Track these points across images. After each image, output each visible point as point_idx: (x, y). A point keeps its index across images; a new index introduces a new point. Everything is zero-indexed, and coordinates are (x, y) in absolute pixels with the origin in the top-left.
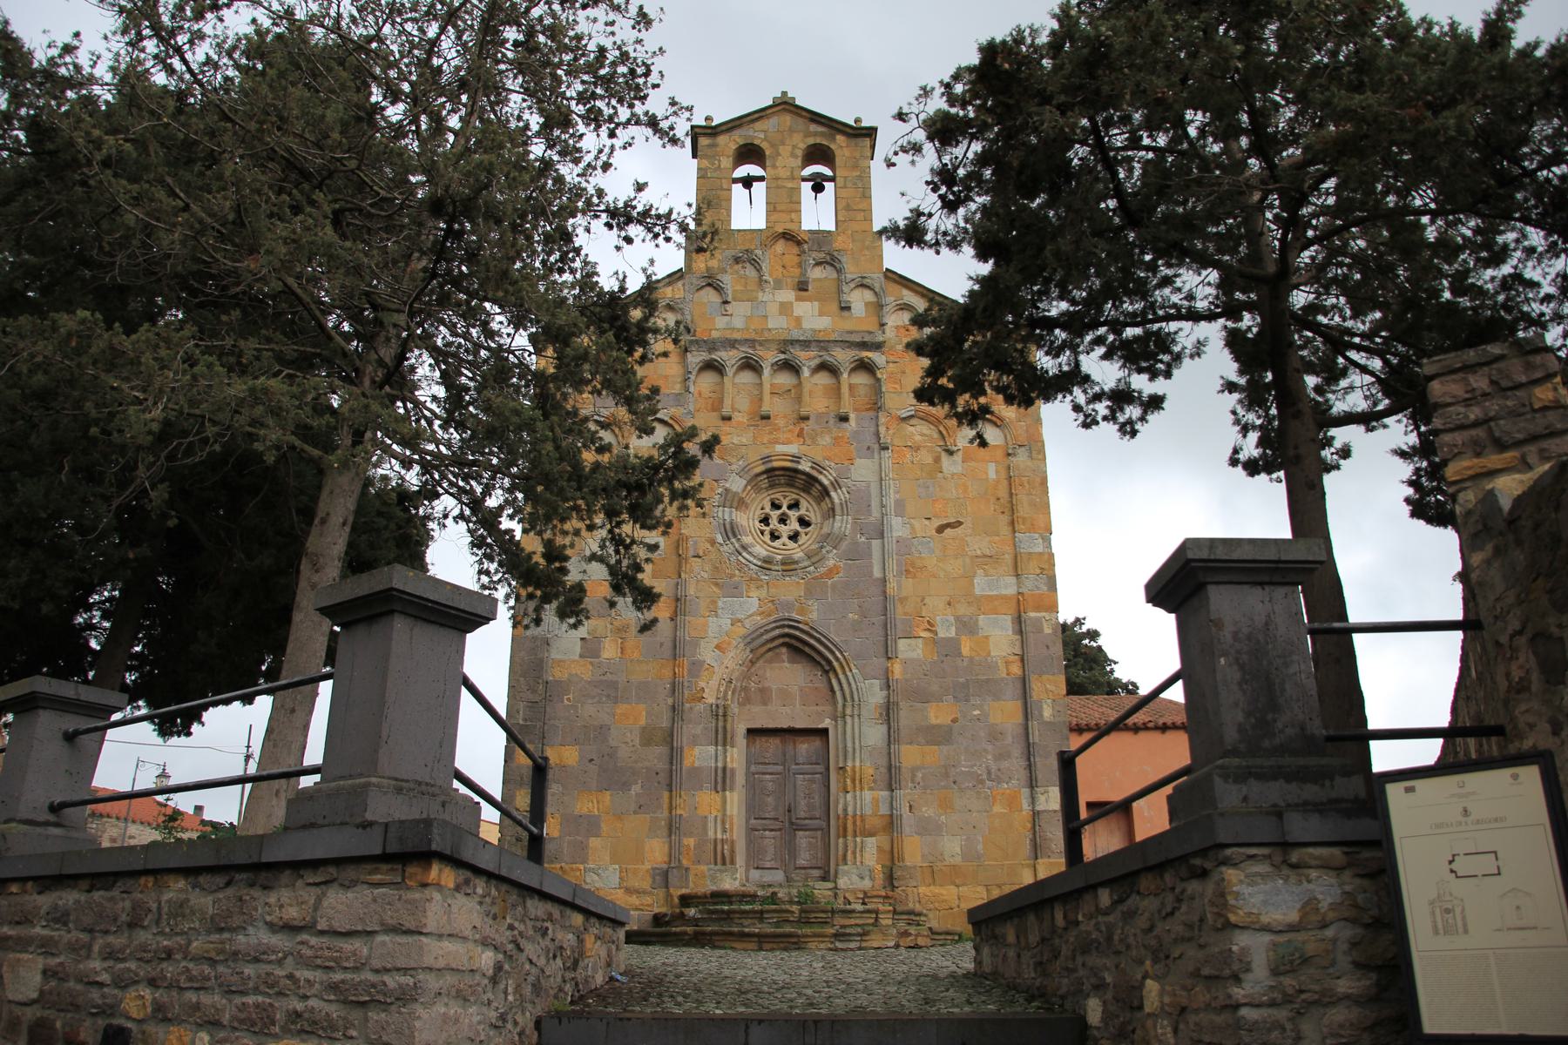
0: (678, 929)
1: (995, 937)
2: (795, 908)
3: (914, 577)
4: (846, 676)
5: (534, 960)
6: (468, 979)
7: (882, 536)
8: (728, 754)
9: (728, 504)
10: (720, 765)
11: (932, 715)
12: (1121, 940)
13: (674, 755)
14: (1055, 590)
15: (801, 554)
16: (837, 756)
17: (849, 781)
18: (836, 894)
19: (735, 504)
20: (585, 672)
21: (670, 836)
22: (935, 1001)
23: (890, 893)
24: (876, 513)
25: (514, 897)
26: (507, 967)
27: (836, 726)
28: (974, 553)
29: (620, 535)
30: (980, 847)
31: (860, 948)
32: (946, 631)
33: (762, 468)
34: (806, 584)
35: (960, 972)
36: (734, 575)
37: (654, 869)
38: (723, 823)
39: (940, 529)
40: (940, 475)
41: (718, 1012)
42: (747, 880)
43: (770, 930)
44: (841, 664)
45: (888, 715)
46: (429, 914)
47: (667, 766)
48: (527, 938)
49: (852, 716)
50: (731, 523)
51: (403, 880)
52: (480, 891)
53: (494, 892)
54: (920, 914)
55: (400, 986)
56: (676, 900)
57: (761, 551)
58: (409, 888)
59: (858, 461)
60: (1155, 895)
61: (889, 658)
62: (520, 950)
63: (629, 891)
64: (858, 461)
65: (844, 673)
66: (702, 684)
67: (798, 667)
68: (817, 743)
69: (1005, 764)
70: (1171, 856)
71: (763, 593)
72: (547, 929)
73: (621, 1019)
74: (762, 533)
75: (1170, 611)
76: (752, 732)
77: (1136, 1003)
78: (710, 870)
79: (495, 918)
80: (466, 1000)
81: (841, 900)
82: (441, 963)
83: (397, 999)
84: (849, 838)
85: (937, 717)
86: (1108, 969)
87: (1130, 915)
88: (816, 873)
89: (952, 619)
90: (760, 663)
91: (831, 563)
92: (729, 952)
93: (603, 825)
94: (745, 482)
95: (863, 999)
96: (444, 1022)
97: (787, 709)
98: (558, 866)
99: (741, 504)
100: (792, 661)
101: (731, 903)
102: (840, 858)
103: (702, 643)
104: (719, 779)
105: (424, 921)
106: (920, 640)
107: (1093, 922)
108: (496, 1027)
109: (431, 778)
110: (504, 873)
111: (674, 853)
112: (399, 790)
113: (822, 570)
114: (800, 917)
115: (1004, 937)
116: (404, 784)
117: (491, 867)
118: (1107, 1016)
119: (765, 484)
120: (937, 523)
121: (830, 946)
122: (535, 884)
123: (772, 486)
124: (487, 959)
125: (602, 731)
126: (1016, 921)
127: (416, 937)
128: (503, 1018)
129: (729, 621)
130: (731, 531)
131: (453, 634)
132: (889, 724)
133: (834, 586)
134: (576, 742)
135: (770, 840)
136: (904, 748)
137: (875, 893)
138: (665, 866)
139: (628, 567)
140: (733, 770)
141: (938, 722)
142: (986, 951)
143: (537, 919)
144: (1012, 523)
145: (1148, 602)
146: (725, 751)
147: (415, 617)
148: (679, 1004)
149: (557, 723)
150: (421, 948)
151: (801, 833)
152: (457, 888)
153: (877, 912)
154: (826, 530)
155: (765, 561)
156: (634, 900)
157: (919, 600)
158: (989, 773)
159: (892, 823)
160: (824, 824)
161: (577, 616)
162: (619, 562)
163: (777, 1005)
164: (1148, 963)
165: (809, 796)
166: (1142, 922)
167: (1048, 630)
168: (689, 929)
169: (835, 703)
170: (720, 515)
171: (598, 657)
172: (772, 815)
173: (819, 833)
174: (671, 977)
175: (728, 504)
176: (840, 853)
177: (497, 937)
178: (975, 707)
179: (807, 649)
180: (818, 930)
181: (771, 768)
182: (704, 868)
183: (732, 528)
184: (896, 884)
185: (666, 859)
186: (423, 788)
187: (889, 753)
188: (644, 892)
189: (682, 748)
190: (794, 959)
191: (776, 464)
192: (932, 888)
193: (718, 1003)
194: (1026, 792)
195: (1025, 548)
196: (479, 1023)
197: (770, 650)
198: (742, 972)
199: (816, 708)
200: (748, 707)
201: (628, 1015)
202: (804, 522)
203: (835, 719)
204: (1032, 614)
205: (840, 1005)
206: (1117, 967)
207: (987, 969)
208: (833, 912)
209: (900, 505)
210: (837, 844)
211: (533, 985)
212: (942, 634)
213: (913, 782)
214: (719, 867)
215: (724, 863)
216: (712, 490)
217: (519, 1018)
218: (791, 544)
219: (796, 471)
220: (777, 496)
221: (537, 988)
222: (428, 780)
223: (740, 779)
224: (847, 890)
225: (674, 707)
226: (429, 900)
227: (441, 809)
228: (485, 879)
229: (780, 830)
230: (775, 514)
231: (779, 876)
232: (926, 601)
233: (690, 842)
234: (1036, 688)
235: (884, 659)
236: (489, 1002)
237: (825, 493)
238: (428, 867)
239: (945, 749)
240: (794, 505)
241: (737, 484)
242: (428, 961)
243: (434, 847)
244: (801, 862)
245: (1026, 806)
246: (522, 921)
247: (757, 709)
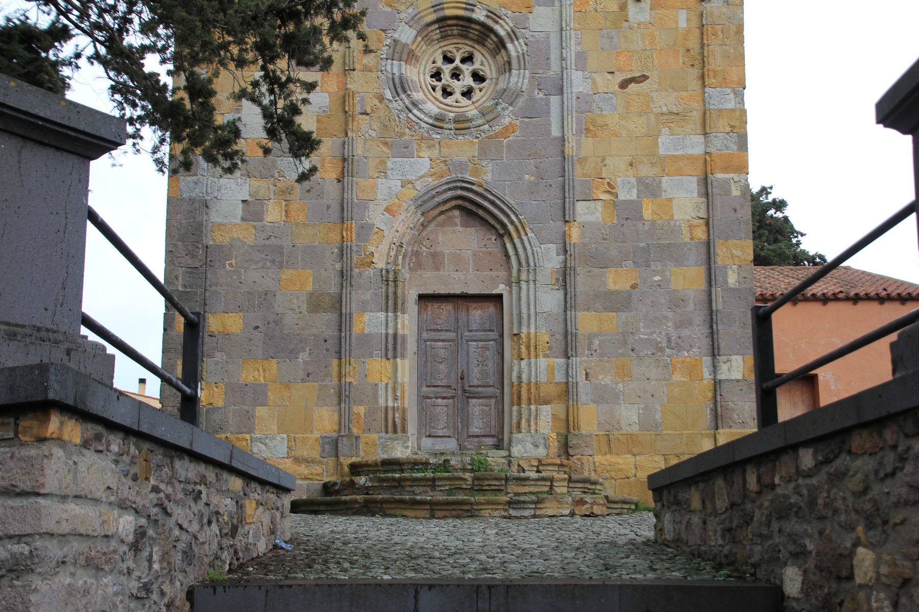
0: (348, 498)
1: (678, 503)
2: (468, 475)
3: (595, 136)
4: (522, 240)
5: (185, 525)
6: (101, 546)
7: (561, 92)
8: (399, 321)
9: (397, 56)
10: (391, 331)
11: (610, 281)
12: (826, 505)
13: (343, 322)
14: (746, 150)
15: (475, 112)
16: (512, 323)
17: (523, 348)
18: (510, 463)
19: (405, 57)
20: (247, 235)
21: (340, 404)
22: (615, 567)
23: (565, 462)
24: (555, 67)
25: (158, 457)
26: (151, 532)
27: (511, 292)
28: (659, 110)
29: (274, 72)
30: (658, 416)
31: (534, 516)
32: (627, 194)
33: (433, 17)
34: (480, 143)
35: (639, 540)
36: (404, 134)
37: (323, 438)
38: (394, 390)
39: (624, 84)
40: (625, 24)
41: (386, 577)
42: (419, 448)
43: (442, 497)
44: (516, 227)
45: (565, 281)
46: (48, 472)
47: (336, 333)
48: (176, 502)
49: (527, 281)
50: (401, 78)
51: (16, 435)
52: (115, 448)
53: (133, 450)
54: (595, 483)
55: (13, 555)
56: (346, 469)
57: (432, 108)
58: (23, 444)
59: (538, 10)
60: (871, 454)
61: (566, 222)
62: (168, 514)
63: (298, 460)
64: (538, 10)
65: (520, 237)
66: (372, 248)
67: (472, 231)
68: (491, 309)
69: (686, 332)
70: (893, 410)
71: (435, 153)
72: (200, 492)
73: (281, 587)
74: (434, 89)
75: (904, 132)
76: (423, 298)
77: (844, 573)
78: (382, 438)
79: (135, 478)
80: (98, 569)
81: (515, 468)
82: (65, 528)
83: (11, 571)
84: (523, 406)
85: (615, 283)
86: (810, 536)
87: (839, 476)
88: (490, 441)
89: (633, 180)
90: (432, 226)
91: (507, 121)
92: (400, 519)
93: (269, 394)
94: (414, 32)
95: (539, 565)
96: (70, 594)
97: (460, 275)
98: (223, 436)
99: (411, 57)
100: (465, 225)
101: (402, 471)
102: (514, 426)
103: (371, 205)
104: (390, 346)
105: (41, 480)
106: (599, 203)
107: (792, 485)
108: (138, 598)
109: (53, 322)
110: (145, 429)
111: (344, 420)
112: (12, 336)
113: (497, 128)
114: (473, 484)
115: (688, 502)
116: (18, 330)
117: (127, 422)
118: (808, 587)
119: (436, 35)
120: (620, 77)
121: (503, 513)
122: (184, 443)
123: (444, 37)
124: (126, 524)
125: (267, 296)
126: (702, 485)
127: (32, 499)
128: (147, 588)
129: (399, 183)
130: (400, 86)
131: (72, 161)
132: (565, 289)
133: (509, 146)
134: (240, 309)
135: (442, 409)
136: (580, 314)
137: (550, 461)
138: (335, 435)
139: (283, 109)
140: (404, 338)
141: (617, 287)
142: (667, 517)
143: (187, 482)
144: (702, 77)
145: (878, 122)
146: (396, 318)
147: (23, 137)
148: (346, 571)
149: (219, 289)
150: (38, 510)
151: (474, 401)
152: (86, 444)
153: (552, 480)
154: (501, 85)
155: (437, 119)
156: (303, 470)
157: (599, 160)
158: (669, 341)
159: (567, 391)
160: (498, 392)
161: (232, 159)
162: (274, 103)
163: (449, 571)
164: (860, 529)
165: (482, 363)
166: (854, 484)
167: (736, 192)
168: (360, 498)
169: (509, 268)
170: (389, 68)
171: (261, 220)
172: (445, 382)
173: (493, 401)
174: (338, 544)
175: (397, 56)
176: (515, 421)
177: (138, 499)
178: (655, 273)
179: (480, 212)
180: (490, 497)
181: (444, 335)
182: (375, 436)
183: (402, 83)
184: (571, 452)
185: (336, 428)
186: (43, 334)
187: (566, 320)
188: (313, 461)
189: (350, 314)
190: (467, 526)
191: (448, 13)
192: (608, 456)
193: (387, 568)
194: (707, 360)
195: (714, 104)
196: (116, 594)
197: (442, 213)
198: (413, 539)
199: (490, 273)
200: (419, 272)
201: (289, 582)
202: (478, 77)
203: (509, 284)
204: (720, 176)
205: (515, 571)
206: (821, 533)
207: (669, 536)
208: (507, 479)
209: (581, 58)
210: (511, 412)
211: (184, 552)
212: (622, 196)
213: (589, 349)
214: (390, 435)
215: (395, 431)
216: (379, 40)
217: (167, 588)
218: (464, 101)
219: (470, 20)
220: (450, 48)
221: (188, 555)
222: (50, 326)
223: (411, 346)
224: (522, 458)
225: (342, 272)
226: (49, 456)
227: (65, 358)
228: (121, 435)
229: (453, 397)
230: (447, 69)
231: (451, 444)
232: (606, 162)
233: (361, 410)
234: (721, 253)
235: (560, 223)
236: (129, 572)
237: (501, 44)
238: (47, 419)
239: (623, 315)
240: (468, 59)
241: (406, 35)
242: (48, 525)
243: (51, 396)
244: (474, 430)
245: (707, 374)
246: (169, 483)
247: (429, 274)
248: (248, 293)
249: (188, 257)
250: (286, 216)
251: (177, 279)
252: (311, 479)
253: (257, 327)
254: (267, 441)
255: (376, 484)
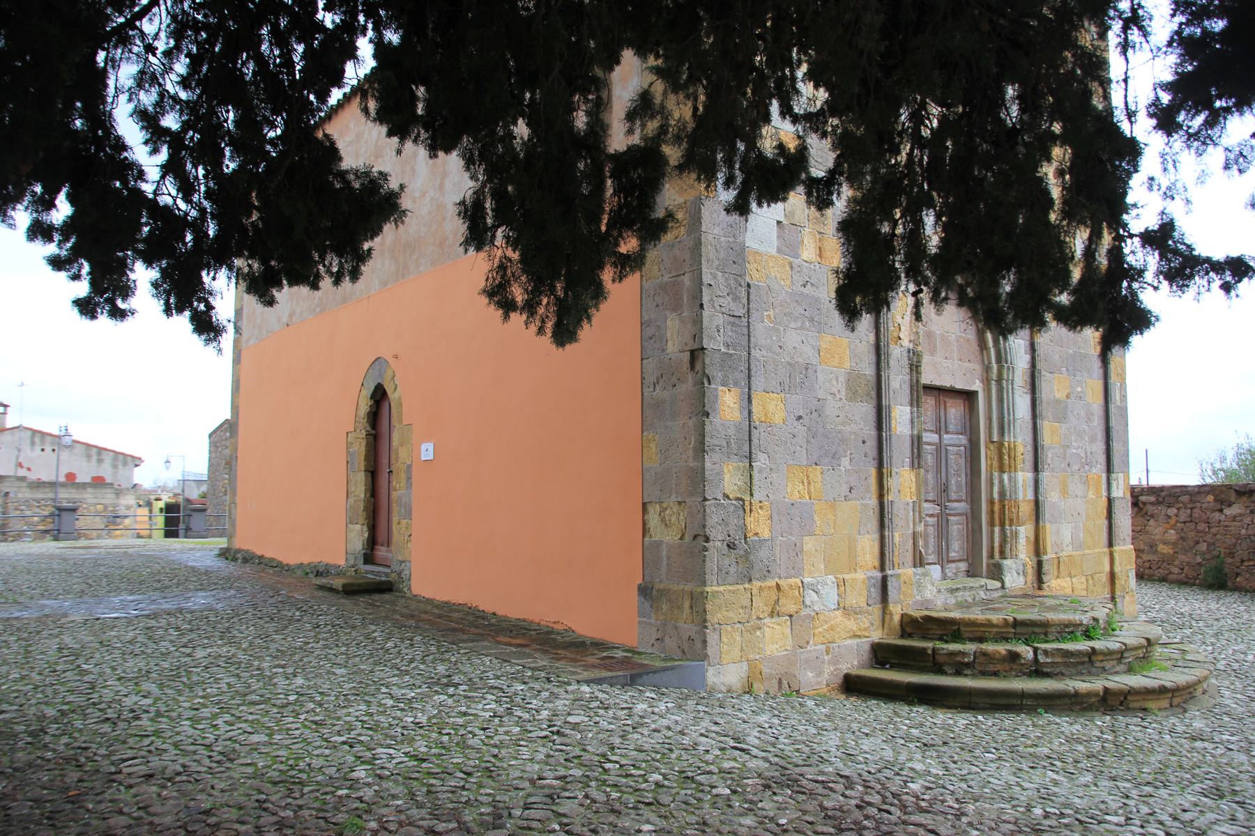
244: (952, 554)
248: (789, 364)
249: (729, 299)
250: (821, 256)
251: (719, 331)
252: (859, 637)
253: (800, 418)
254: (819, 587)
255: (1059, 660)
